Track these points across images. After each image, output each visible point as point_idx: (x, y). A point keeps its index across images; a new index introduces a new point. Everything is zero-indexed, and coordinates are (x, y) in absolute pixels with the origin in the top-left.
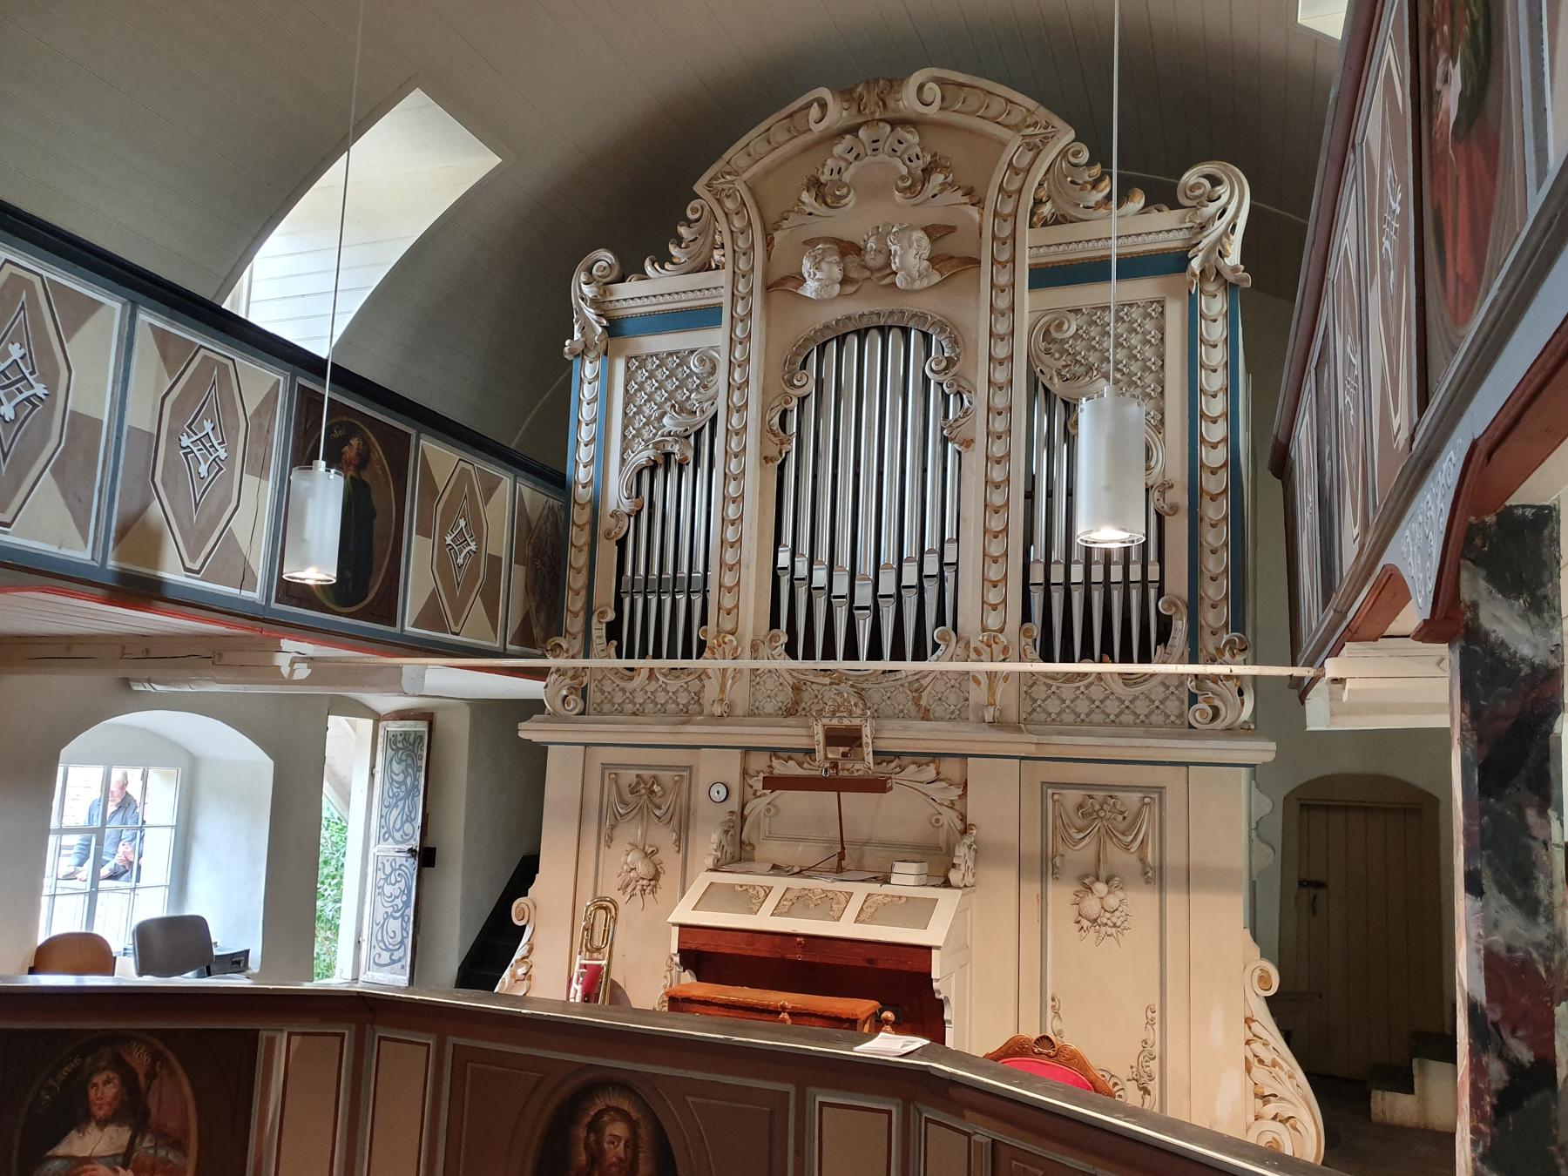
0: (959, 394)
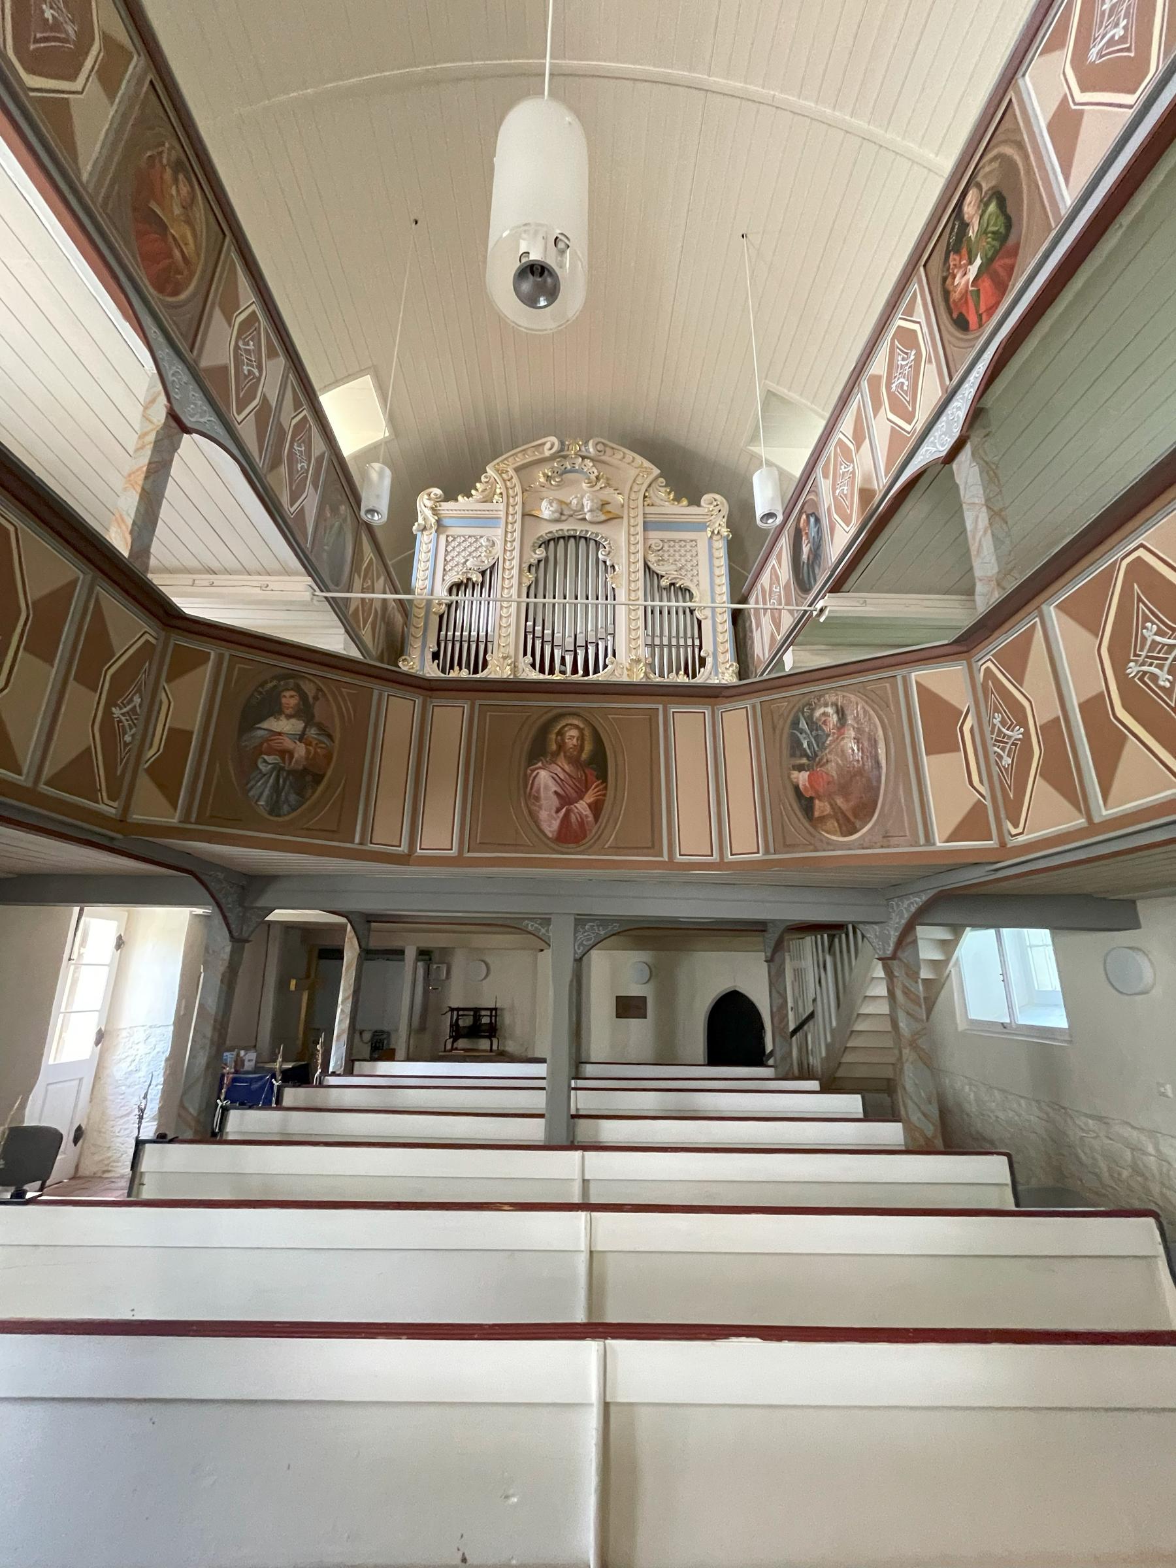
0: (613, 566)
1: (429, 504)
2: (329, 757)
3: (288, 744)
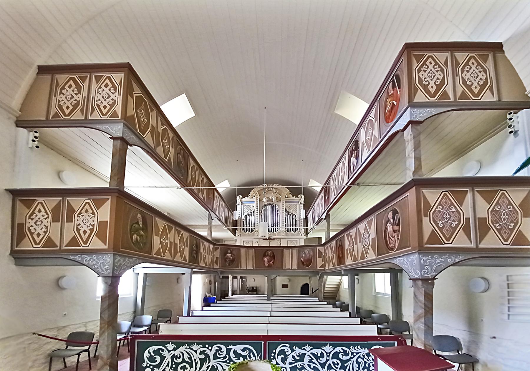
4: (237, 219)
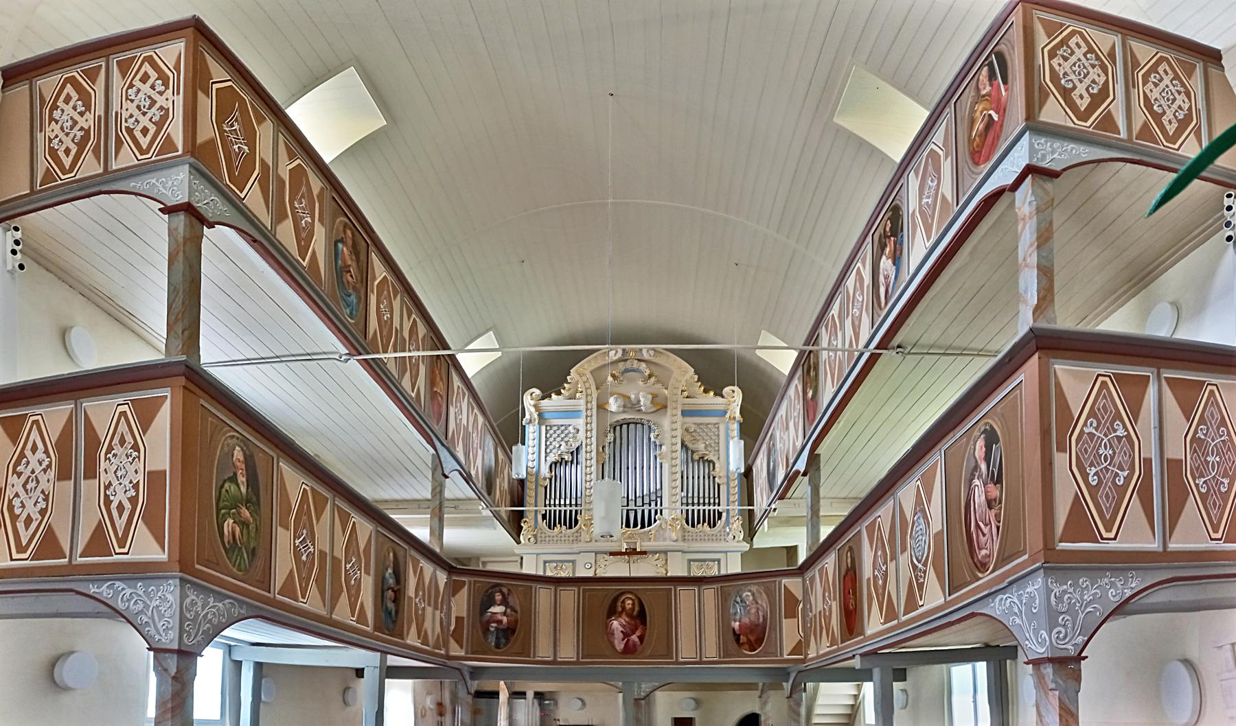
1: (532, 402)
2: (516, 621)
3: (500, 617)
4: (523, 475)
